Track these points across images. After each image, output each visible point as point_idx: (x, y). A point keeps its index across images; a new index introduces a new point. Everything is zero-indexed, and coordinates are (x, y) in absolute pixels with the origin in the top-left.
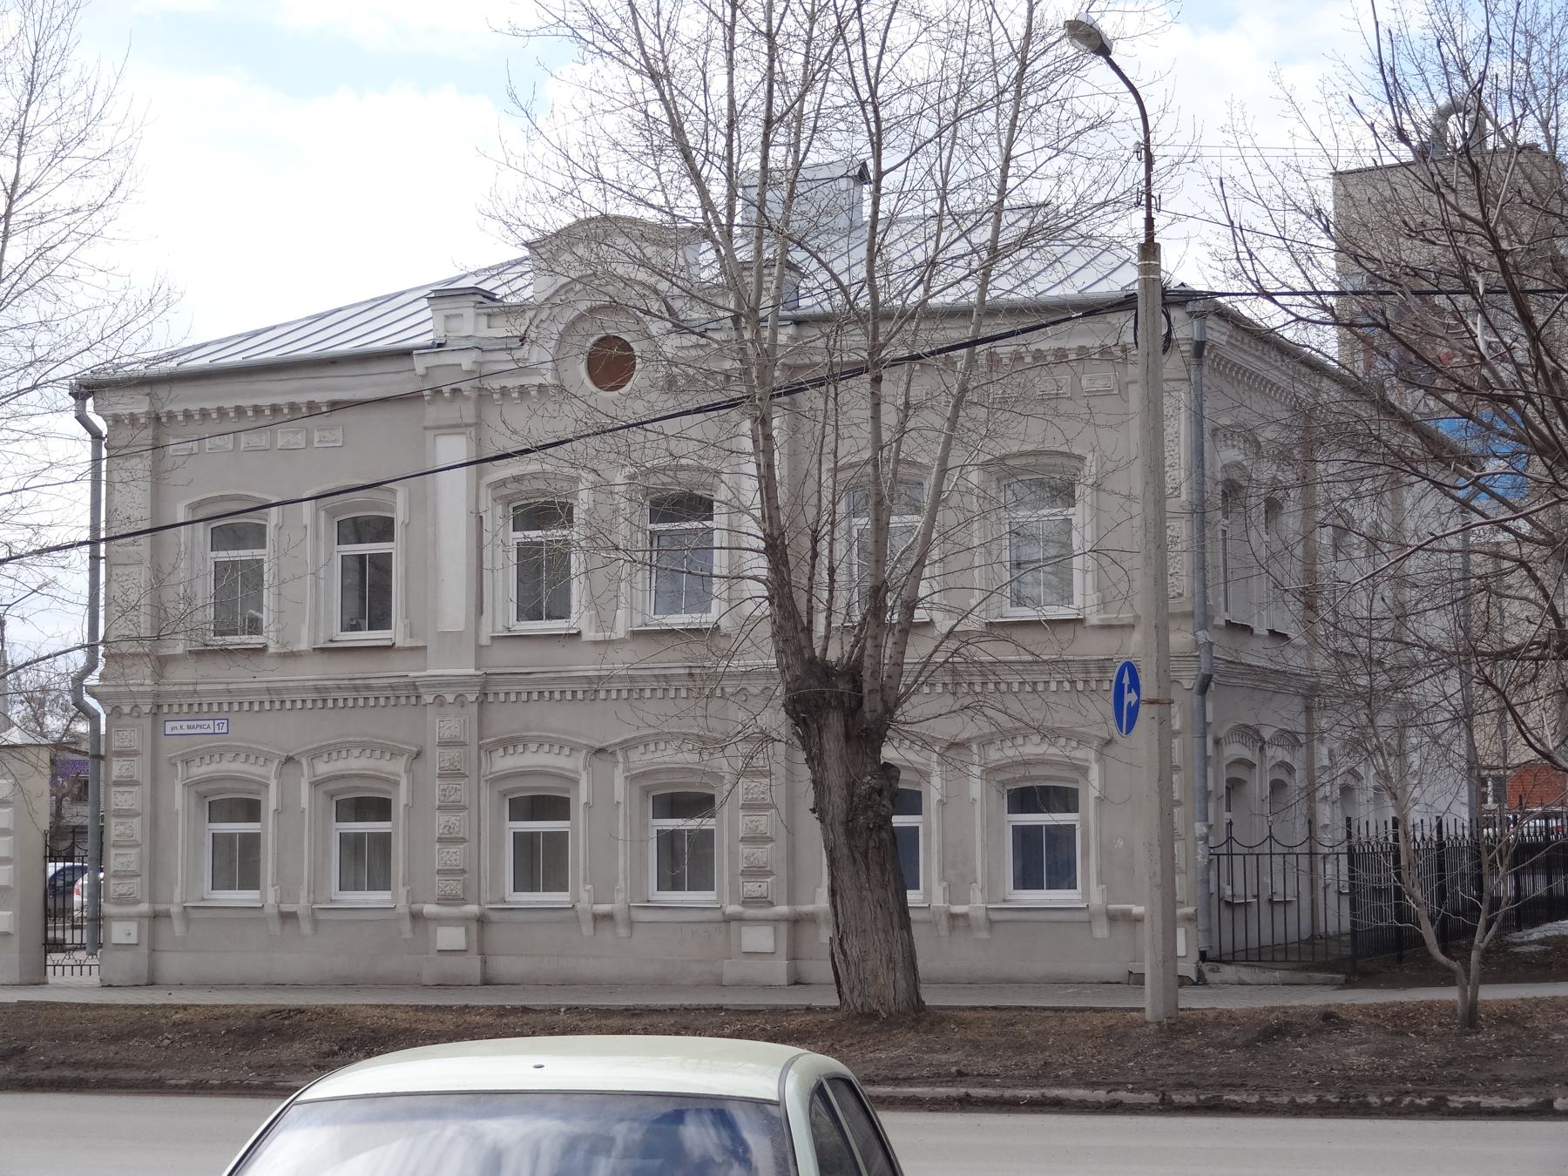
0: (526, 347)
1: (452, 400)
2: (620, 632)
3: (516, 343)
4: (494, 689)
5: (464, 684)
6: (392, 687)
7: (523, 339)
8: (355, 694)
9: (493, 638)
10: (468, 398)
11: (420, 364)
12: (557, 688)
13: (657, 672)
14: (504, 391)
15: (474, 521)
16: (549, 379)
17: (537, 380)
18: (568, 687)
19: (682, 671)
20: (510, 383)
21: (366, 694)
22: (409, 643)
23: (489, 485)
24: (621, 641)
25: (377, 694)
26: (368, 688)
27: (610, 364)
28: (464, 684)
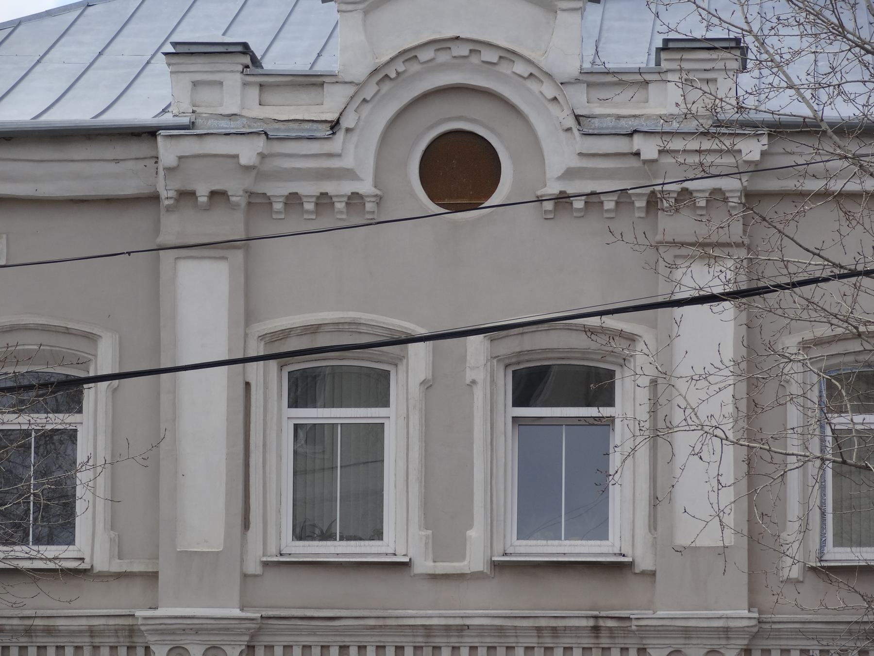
0: (340, 136)
2: (475, 560)
4: (267, 640)
5: (226, 630)
6: (92, 632)
7: (335, 125)
8: (23, 641)
9: (266, 564)
10: (235, 207)
11: (168, 151)
12: (371, 641)
13: (543, 623)
14: (293, 200)
15: (241, 387)
16: (366, 187)
17: (347, 187)
18: (391, 641)
19: (584, 623)
20: (308, 189)
21: (42, 641)
22: (117, 566)
23: (262, 337)
24: (476, 576)
25: (61, 641)
26: (49, 631)
27: (460, 171)
28: (226, 630)
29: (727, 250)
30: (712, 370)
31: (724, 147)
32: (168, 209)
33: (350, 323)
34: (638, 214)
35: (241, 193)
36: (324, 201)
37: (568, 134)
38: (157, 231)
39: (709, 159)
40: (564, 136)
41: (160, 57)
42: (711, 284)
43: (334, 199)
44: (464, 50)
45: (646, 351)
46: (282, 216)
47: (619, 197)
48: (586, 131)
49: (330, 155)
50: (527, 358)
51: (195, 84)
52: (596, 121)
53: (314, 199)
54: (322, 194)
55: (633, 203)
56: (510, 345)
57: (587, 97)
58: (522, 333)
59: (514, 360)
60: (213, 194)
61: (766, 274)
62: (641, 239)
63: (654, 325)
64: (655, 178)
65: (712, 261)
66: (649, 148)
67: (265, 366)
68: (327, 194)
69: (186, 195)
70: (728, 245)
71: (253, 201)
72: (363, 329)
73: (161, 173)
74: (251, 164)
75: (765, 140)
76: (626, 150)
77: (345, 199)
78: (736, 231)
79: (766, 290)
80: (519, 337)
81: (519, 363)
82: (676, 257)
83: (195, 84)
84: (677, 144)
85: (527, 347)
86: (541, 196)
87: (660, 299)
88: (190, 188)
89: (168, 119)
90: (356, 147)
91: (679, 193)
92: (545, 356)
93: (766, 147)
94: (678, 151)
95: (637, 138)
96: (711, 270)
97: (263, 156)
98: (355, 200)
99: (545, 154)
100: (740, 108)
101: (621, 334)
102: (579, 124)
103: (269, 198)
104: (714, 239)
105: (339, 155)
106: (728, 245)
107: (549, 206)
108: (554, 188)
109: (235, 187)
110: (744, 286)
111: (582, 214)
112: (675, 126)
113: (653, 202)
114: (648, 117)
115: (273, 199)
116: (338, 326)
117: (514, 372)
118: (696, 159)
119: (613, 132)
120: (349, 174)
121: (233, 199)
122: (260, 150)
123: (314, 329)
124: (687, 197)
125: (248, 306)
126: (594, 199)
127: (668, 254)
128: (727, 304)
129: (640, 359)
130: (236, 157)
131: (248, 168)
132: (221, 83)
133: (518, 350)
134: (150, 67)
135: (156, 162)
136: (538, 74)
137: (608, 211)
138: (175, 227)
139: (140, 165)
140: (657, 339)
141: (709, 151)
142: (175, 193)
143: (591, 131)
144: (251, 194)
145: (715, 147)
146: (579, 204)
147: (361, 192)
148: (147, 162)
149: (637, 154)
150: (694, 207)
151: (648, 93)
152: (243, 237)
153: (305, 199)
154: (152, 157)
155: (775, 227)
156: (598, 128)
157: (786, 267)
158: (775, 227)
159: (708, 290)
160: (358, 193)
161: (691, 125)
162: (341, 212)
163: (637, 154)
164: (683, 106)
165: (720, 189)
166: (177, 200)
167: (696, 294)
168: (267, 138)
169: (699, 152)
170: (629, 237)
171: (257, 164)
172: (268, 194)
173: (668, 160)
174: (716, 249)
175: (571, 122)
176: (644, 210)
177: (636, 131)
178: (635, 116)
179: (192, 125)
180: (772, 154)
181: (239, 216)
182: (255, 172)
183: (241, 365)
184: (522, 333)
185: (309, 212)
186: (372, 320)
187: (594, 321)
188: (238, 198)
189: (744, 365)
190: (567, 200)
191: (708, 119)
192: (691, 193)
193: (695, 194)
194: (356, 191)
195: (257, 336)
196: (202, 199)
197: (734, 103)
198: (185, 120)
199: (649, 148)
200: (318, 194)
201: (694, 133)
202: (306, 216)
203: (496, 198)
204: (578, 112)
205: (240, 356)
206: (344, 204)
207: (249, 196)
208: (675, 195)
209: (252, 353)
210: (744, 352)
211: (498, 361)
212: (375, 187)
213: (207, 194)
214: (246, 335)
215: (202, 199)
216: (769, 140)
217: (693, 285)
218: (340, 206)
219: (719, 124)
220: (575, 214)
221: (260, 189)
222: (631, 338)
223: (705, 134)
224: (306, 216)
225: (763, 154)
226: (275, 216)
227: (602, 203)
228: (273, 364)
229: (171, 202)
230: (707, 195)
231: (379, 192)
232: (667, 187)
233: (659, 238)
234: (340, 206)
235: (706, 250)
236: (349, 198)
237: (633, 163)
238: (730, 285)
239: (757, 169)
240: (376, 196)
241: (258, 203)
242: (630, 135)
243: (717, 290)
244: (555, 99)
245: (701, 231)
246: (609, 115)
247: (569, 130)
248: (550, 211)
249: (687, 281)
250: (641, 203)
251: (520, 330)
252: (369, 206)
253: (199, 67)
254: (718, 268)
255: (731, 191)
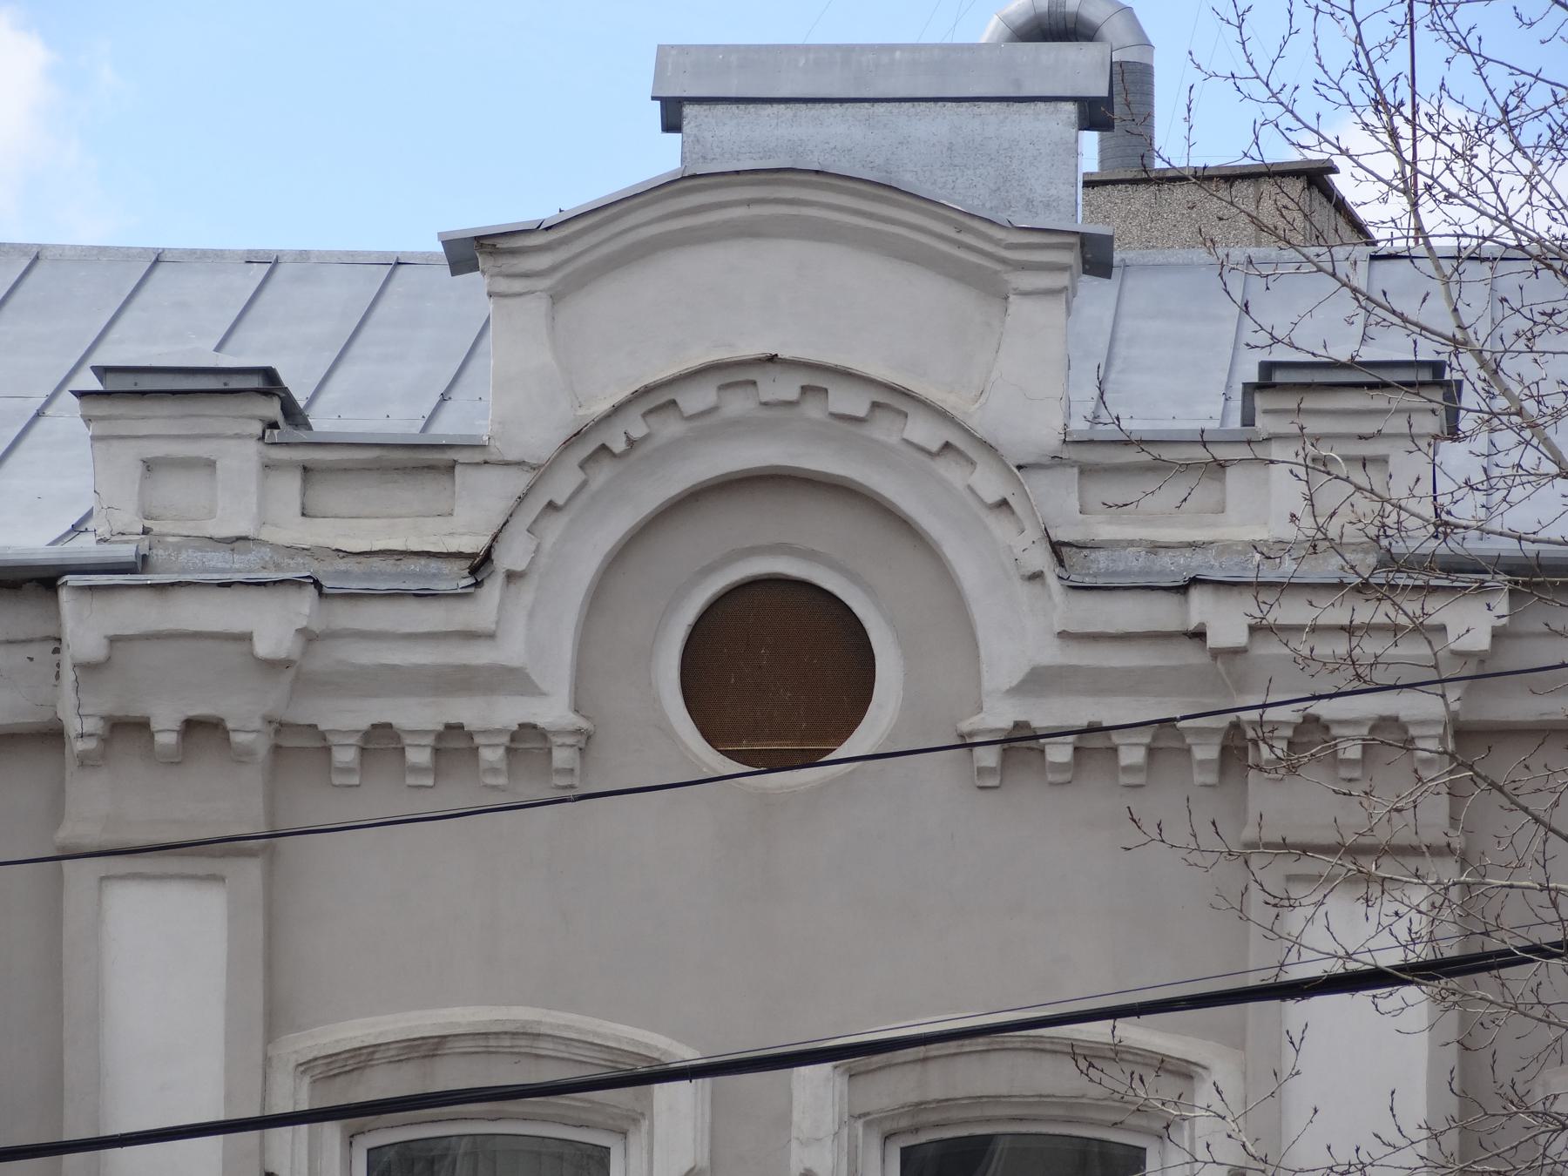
0: (493, 589)
1: (176, 760)
3: (454, 577)
7: (480, 565)
10: (242, 756)
11: (84, 624)
14: (381, 741)
16: (553, 711)
17: (509, 712)
20: (418, 715)
23: (306, 1066)
27: (778, 674)
29: (1412, 863)
30: (1378, 1150)
31: (1402, 620)
32: (84, 761)
33: (514, 1034)
34: (1199, 778)
35: (257, 723)
36: (454, 744)
37: (1035, 587)
38: (56, 811)
39: (1370, 647)
40: (1024, 591)
41: (68, 400)
42: (1372, 945)
43: (478, 740)
44: (785, 387)
45: (1218, 1106)
46: (355, 780)
47: (1155, 738)
48: (1076, 579)
49: (470, 636)
50: (934, 1117)
51: (149, 465)
52: (1101, 555)
53: (430, 740)
54: (449, 727)
55: (1188, 751)
56: (896, 1087)
57: (1081, 498)
58: (925, 1060)
59: (904, 1123)
60: (192, 726)
61: (1506, 921)
62: (1207, 838)
63: (1236, 1040)
64: (1241, 690)
65: (1375, 890)
66: (1226, 622)
67: (310, 1134)
68: (460, 727)
69: (127, 729)
70: (1414, 851)
71: (287, 742)
72: (545, 1048)
73: (68, 676)
74: (282, 655)
75: (1502, 604)
76: (1173, 626)
77: (505, 739)
78: (1434, 817)
79: (1506, 959)
80: (918, 1067)
81: (916, 1130)
82: (1290, 878)
83: (149, 465)
84: (1292, 611)
85: (936, 1092)
86: (971, 734)
87: (1253, 981)
88: (136, 711)
89: (85, 547)
90: (531, 615)
91: (1297, 728)
92: (976, 1113)
93: (1504, 621)
94: (1298, 629)
95: (1196, 595)
96: (1373, 912)
97: (308, 637)
98: (527, 741)
99: (981, 634)
100: (1443, 526)
101: (1164, 1065)
102: (1061, 563)
103: (323, 736)
104: (1382, 837)
105: (491, 636)
106: (1414, 851)
107: (988, 757)
108: (1000, 716)
109: (244, 710)
110: (1451, 950)
111: (1067, 776)
112: (1287, 568)
113: (1236, 749)
114: (1226, 548)
115: (333, 739)
116: (485, 1041)
117: (906, 1153)
118: (1342, 648)
119: (1142, 581)
120: (513, 680)
121: (237, 738)
122: (302, 623)
123: (429, 1048)
124: (1318, 737)
125: (272, 994)
126: (1095, 741)
127: (1273, 873)
128: (1410, 993)
129: (1204, 1125)
130: (246, 638)
131: (274, 666)
132: (211, 464)
133: (913, 1098)
134: (43, 424)
135: (56, 651)
136: (963, 444)
137: (1128, 769)
138: (99, 804)
139: (19, 656)
140: (1245, 1074)
141: (1369, 628)
142: (101, 723)
143: (1088, 581)
144: (282, 728)
145: (1380, 619)
146: (1059, 752)
147: (541, 722)
148: (33, 650)
149: (1199, 635)
150: (1335, 761)
151: (1223, 491)
152: (262, 829)
153: (408, 740)
154: (46, 639)
155: (1526, 810)
156: (1108, 573)
157: (1555, 905)
158: (1526, 810)
159: (1367, 958)
160: (534, 727)
161: (1328, 568)
162: (494, 771)
163: (1199, 635)
164: (1307, 522)
165: (1396, 719)
166: (105, 741)
167: (1336, 967)
168: (321, 594)
169: (1349, 630)
170: (1178, 833)
171: (295, 656)
172: (322, 727)
173: (1271, 648)
174: (1386, 861)
175: (1041, 559)
176: (1216, 767)
177: (1195, 581)
178: (1193, 546)
179: (142, 563)
180: (1517, 636)
181: (252, 778)
182: (291, 672)
183: (256, 1133)
184: (925, 1060)
185: (417, 770)
186: (567, 1027)
187: (1097, 1031)
188: (251, 737)
189: (1451, 1141)
190: (1032, 744)
191: (1366, 552)
192: (1326, 728)
193: (1335, 731)
194: (532, 721)
195: (292, 1065)
196: (166, 739)
197: (1429, 512)
198: (125, 552)
199: (1226, 622)
200: (440, 728)
201: (1341, 585)
202: (411, 780)
204: (1059, 535)
205: (253, 1112)
206: (501, 752)
207: (277, 732)
208: (1289, 733)
209: (282, 1105)
210: (1452, 1105)
211: (867, 1125)
212: (576, 711)
213: (176, 726)
214: (267, 1061)
215: (166, 739)
217: (1331, 947)
218: (492, 755)
219: (1389, 561)
220: (1050, 777)
221: (303, 714)
222: (1185, 1071)
223: (1363, 588)
224: (411, 780)
225: (1497, 635)
226: (337, 780)
227: (1114, 750)
228: (331, 1131)
229: (91, 744)
230: (1364, 731)
231: (584, 724)
232: (1272, 714)
233: (1250, 833)
234: (492, 755)
235: (1361, 862)
236: (514, 737)
237: (1190, 655)
238: (1418, 948)
239: (1480, 673)
240: (578, 732)
241: (298, 747)
242: (1183, 589)
243: (1389, 958)
244: (1004, 503)
245: (1352, 821)
246: (1131, 543)
247: (1036, 576)
248: (991, 771)
249: (1316, 937)
250: (1207, 752)
251: (920, 1051)
252: (561, 757)
253: (160, 428)
254: (1390, 907)
255: (1423, 723)
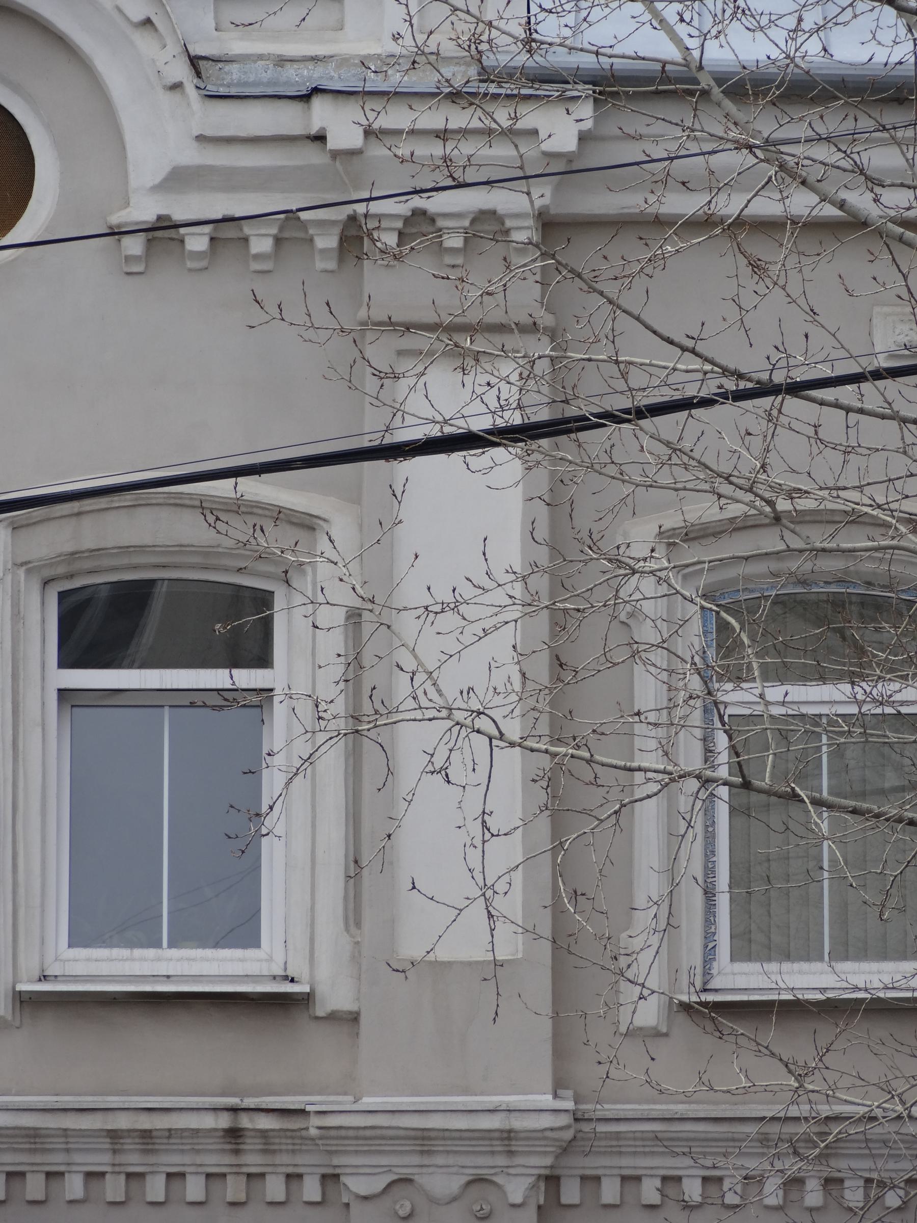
29: (498, 339)
30: (467, 591)
31: (494, 126)
34: (320, 265)
37: (176, 96)
39: (467, 148)
40: (166, 100)
42: (465, 412)
45: (330, 553)
47: (281, 229)
48: (212, 89)
50: (88, 565)
52: (234, 67)
55: (311, 240)
56: (54, 538)
57: (216, 17)
58: (79, 514)
59: (61, 570)
61: (582, 392)
62: (321, 317)
63: (354, 496)
64: (357, 188)
65: (470, 362)
66: (342, 126)
70: (501, 328)
75: (586, 110)
76: (298, 130)
78: (525, 299)
79: (582, 424)
80: (73, 521)
81: (71, 576)
82: (400, 353)
84: (396, 117)
85: (89, 542)
86: (119, 226)
87: (365, 443)
91: (407, 221)
92: (125, 561)
93: (588, 125)
94: (398, 132)
95: (317, 103)
96: (468, 380)
99: (128, 137)
100: (530, 42)
101: (280, 515)
102: (198, 74)
104: (473, 317)
106: (501, 328)
107: (134, 245)
108: (144, 211)
110: (543, 415)
111: (204, 263)
112: (396, 79)
113: (354, 238)
114: (344, 61)
117: (62, 596)
118: (437, 149)
119: (270, 91)
124: (425, 228)
126: (229, 232)
127: (381, 351)
128: (498, 453)
129: (324, 570)
133: (69, 548)
137: (258, 257)
140: (361, 526)
141: (465, 133)
143: (223, 91)
145: (476, 124)
146: (197, 242)
149: (320, 138)
150: (441, 250)
151: (342, 11)
155: (601, 293)
156: (240, 84)
157: (624, 376)
158: (601, 293)
159: (461, 423)
161: (425, 80)
163: (320, 138)
164: (408, 41)
165: (494, 212)
167: (434, 431)
169: (443, 135)
170: (294, 313)
173: (378, 151)
174: (478, 337)
175: (181, 71)
176: (335, 254)
177: (316, 90)
178: (315, 59)
180: (603, 139)
184: (79, 514)
187: (223, 488)
189: (541, 583)
190: (171, 233)
191: (468, 65)
192: (433, 220)
193: (441, 223)
197: (520, 33)
199: (342, 126)
201: (433, 95)
203: (22, 231)
204: (197, 49)
208: (399, 224)
210: (542, 555)
211: (29, 572)
216: (595, 111)
217: (429, 413)
219: (486, 75)
220: (190, 264)
222: (307, 524)
223: (455, 96)
225: (583, 138)
227: (246, 240)
230: (467, 223)
232: (376, 207)
233: (362, 314)
235: (459, 339)
237: (312, 156)
238: (507, 415)
239: (568, 170)
242: (306, 98)
243: (480, 424)
244: (148, 22)
245: (447, 302)
246: (261, 57)
247: (177, 87)
248: (136, 259)
249: (417, 405)
250: (328, 241)
251: (74, 506)
254: (483, 379)
255: (517, 216)
